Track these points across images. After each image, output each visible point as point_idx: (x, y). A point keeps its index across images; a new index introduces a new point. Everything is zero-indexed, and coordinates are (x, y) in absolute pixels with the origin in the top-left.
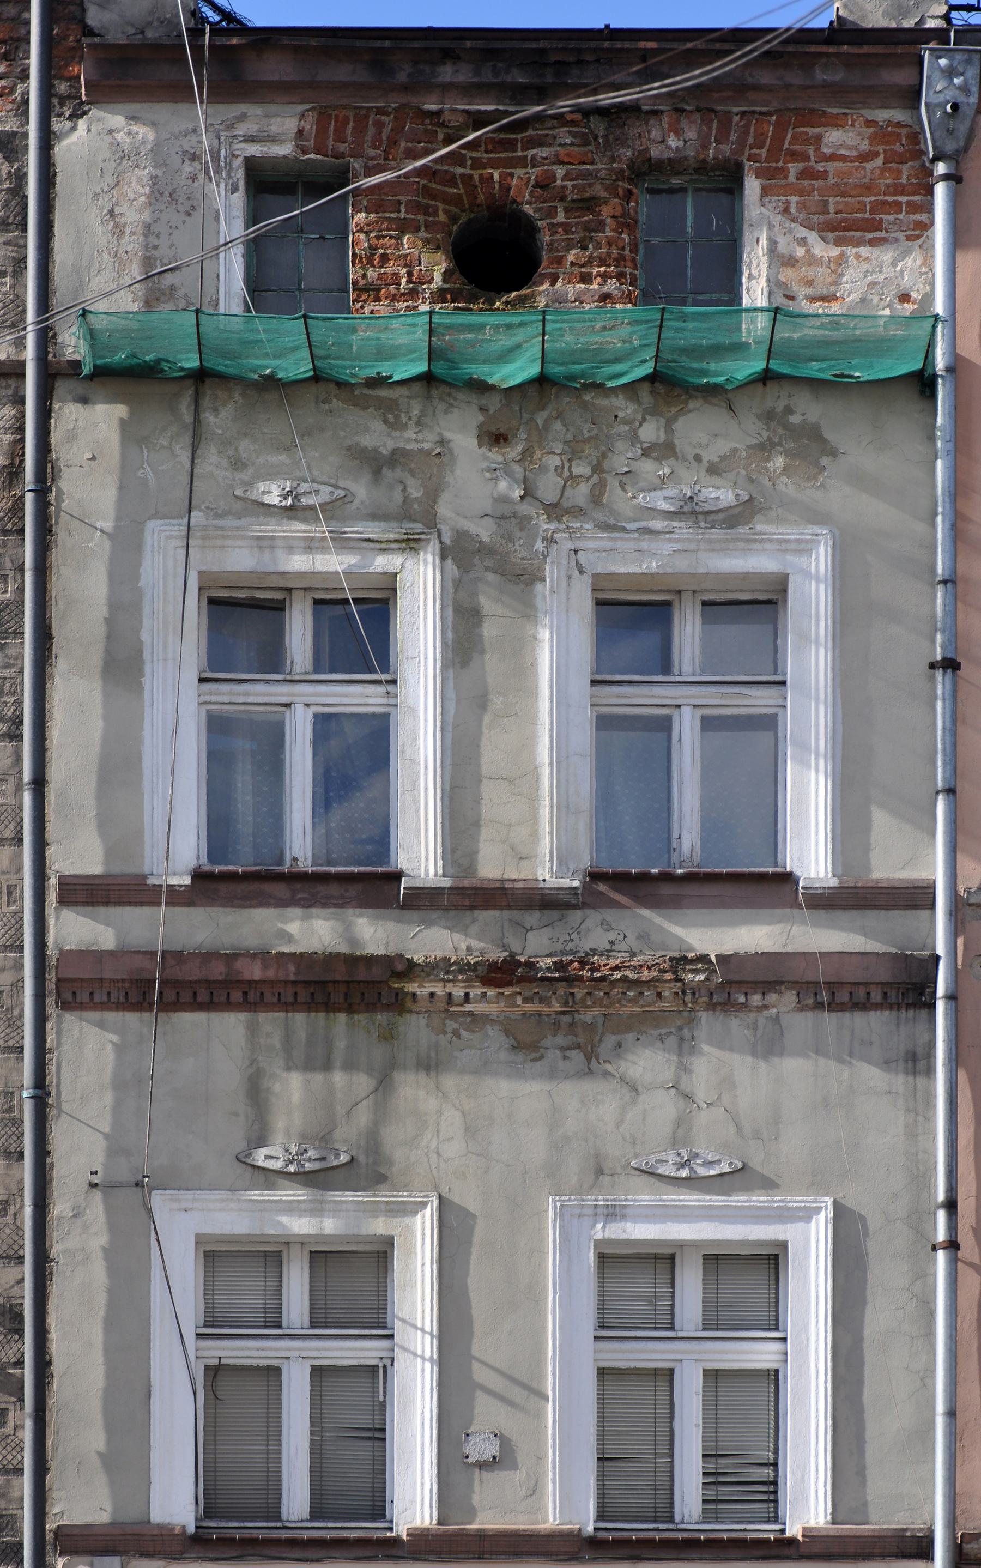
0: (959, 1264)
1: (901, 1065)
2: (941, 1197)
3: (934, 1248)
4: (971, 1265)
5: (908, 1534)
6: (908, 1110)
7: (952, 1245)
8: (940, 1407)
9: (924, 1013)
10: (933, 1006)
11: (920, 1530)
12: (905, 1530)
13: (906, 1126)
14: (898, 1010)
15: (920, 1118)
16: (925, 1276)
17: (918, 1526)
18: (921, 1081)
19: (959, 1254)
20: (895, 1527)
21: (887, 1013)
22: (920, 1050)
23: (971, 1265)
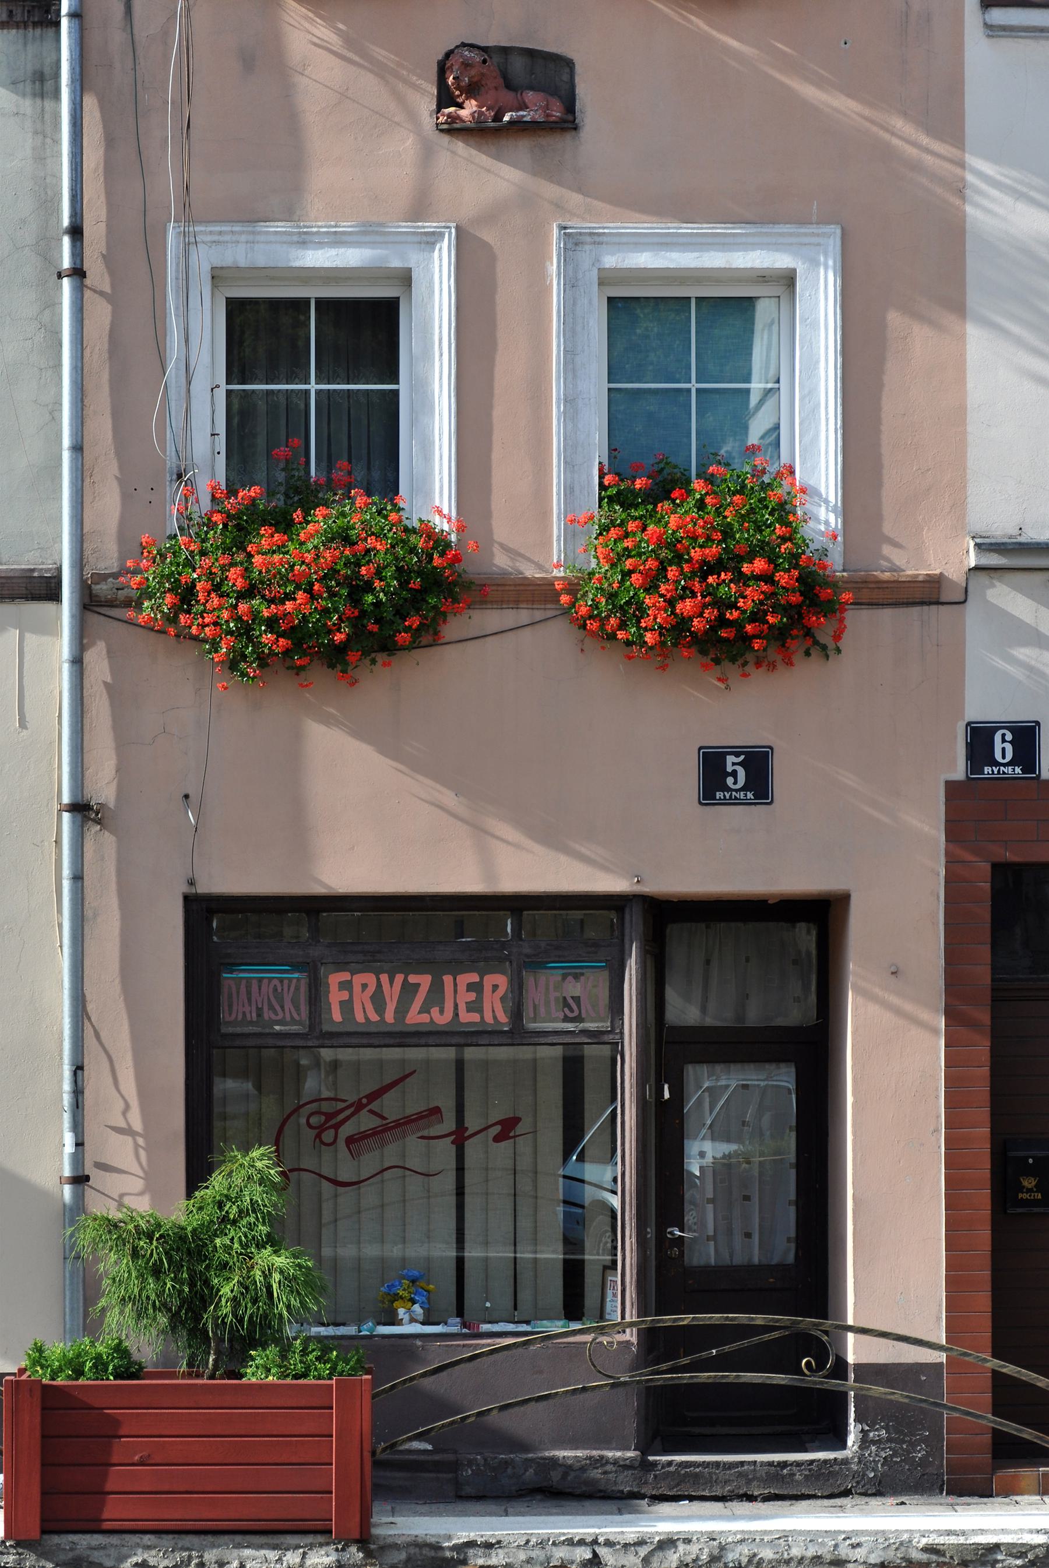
0: (88, 294)
1: (29, 88)
2: (66, 222)
3: (60, 276)
4: (102, 293)
5: (36, 574)
6: (36, 133)
7: (78, 273)
8: (66, 442)
9: (51, 32)
10: (57, 24)
11: (48, 570)
12: (33, 570)
13: (34, 149)
14: (25, 28)
15: (48, 141)
16: (54, 305)
17: (46, 566)
18: (48, 104)
19: (88, 281)
20: (23, 567)
21: (14, 31)
22: (47, 70)
23: (102, 293)
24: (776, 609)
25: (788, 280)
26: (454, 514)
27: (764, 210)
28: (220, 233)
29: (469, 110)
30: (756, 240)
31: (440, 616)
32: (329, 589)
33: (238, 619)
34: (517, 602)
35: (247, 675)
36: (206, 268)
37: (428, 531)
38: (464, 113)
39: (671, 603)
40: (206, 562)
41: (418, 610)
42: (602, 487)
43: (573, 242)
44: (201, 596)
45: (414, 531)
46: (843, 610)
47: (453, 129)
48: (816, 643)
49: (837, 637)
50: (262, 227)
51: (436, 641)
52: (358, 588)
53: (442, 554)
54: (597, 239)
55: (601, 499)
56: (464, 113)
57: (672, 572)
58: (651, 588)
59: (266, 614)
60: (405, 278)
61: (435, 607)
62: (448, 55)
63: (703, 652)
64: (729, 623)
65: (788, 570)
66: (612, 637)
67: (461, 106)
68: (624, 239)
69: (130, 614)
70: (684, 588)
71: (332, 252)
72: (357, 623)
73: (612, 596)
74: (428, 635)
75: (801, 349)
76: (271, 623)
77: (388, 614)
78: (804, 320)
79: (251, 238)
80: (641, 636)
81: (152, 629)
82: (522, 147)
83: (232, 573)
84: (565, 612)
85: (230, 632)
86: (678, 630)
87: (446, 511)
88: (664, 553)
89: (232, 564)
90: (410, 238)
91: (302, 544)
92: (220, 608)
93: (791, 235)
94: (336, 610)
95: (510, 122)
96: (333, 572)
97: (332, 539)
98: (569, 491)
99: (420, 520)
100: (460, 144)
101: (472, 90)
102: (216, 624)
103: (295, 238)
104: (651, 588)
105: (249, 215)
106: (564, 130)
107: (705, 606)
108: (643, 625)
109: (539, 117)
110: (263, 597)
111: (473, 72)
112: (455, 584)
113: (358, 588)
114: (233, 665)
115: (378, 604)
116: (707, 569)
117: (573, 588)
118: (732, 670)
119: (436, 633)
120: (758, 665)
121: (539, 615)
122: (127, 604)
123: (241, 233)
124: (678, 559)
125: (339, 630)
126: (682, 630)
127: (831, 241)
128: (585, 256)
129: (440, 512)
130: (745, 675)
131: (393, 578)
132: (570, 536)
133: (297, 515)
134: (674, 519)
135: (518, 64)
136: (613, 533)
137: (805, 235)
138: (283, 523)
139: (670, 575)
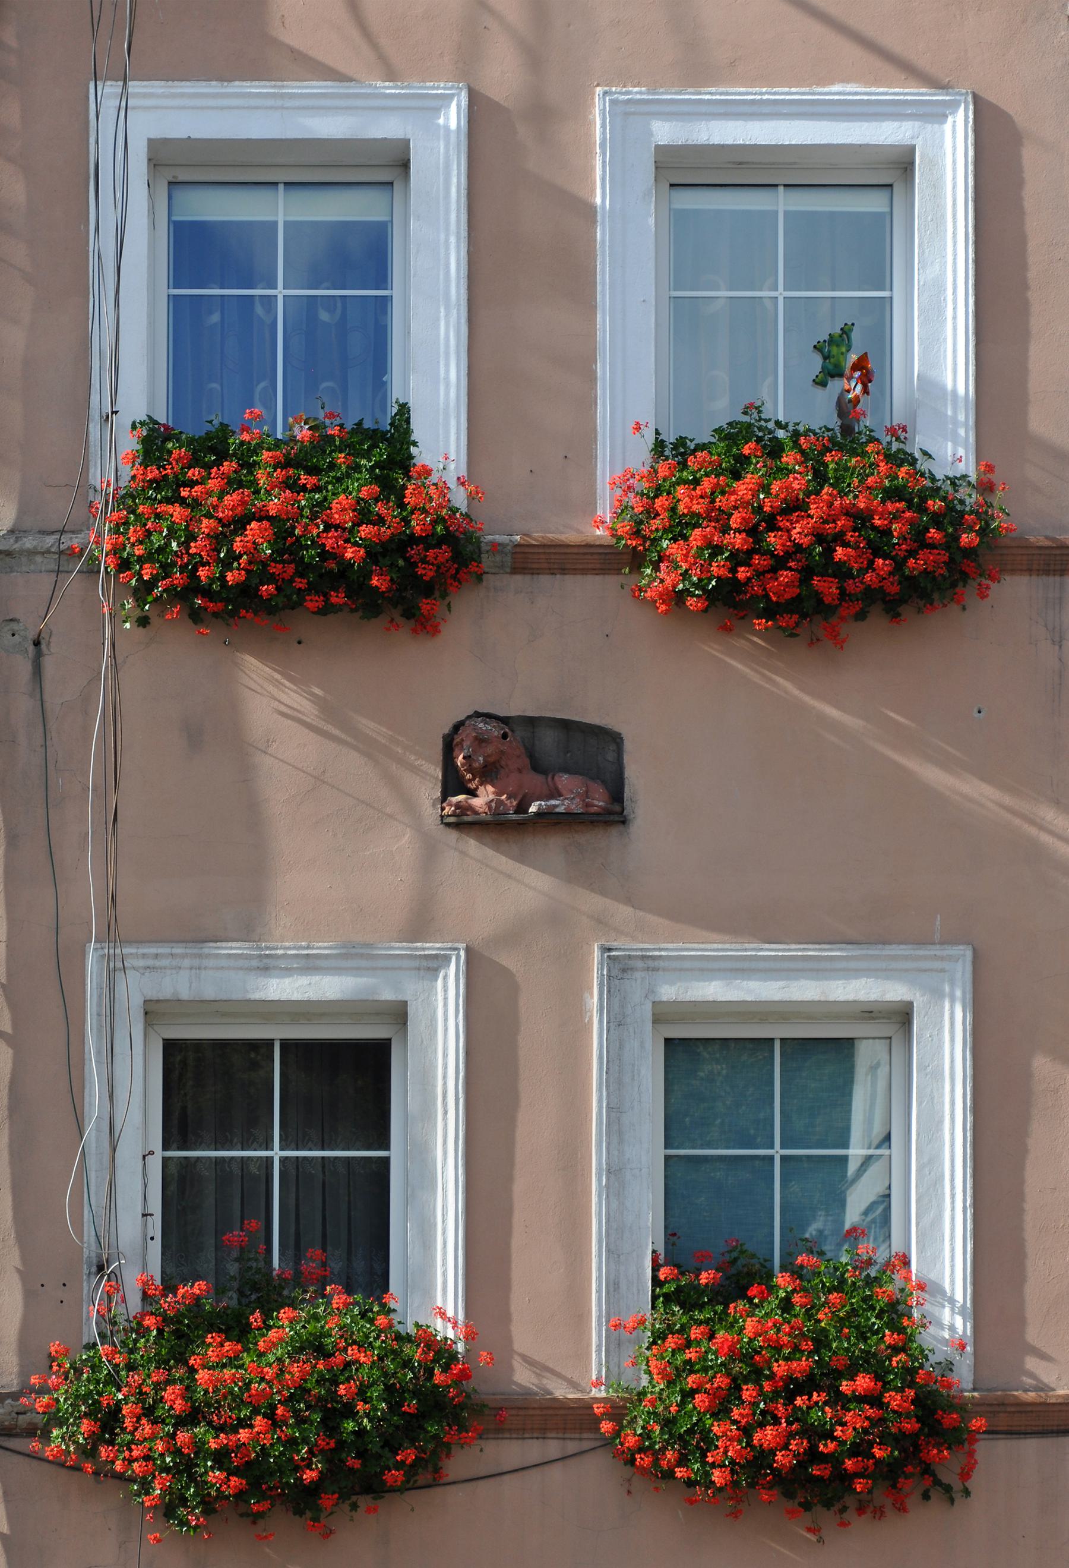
24: (884, 1439)
25: (902, 1017)
26: (461, 1317)
27: (871, 927)
28: (156, 956)
29: (484, 798)
30: (863, 965)
31: (442, 1448)
32: (296, 1413)
33: (177, 1452)
34: (544, 1430)
35: (187, 1523)
36: (137, 1002)
37: (426, 1339)
38: (478, 802)
39: (746, 1431)
40: (135, 1378)
41: (413, 1441)
42: (656, 1282)
43: (620, 968)
44: (128, 1423)
45: (409, 1338)
46: (972, 1440)
47: (463, 823)
48: (937, 1482)
49: (965, 1475)
50: (210, 948)
51: (437, 1480)
52: (335, 1413)
53: (446, 1368)
54: (651, 964)
55: (654, 1298)
56: (478, 802)
57: (748, 1392)
58: (720, 1412)
59: (213, 1446)
60: (399, 1014)
61: (436, 1437)
62: (457, 727)
63: (789, 1495)
64: (823, 1458)
65: (901, 1390)
66: (669, 1475)
67: (473, 793)
68: (687, 964)
69: (34, 1445)
70: (763, 1413)
71: (303, 981)
72: (333, 1458)
73: (668, 1423)
74: (427, 1473)
75: (919, 1104)
76: (220, 1458)
77: (374, 1445)
78: (922, 1068)
79: (196, 962)
80: (707, 1474)
81: (63, 1465)
82: (554, 846)
83: (169, 1393)
84: (607, 1443)
85: (166, 1469)
86: (756, 1465)
87: (450, 1313)
88: (737, 1368)
89: (169, 1382)
90: (406, 963)
91: (261, 1355)
92: (153, 1437)
93: (906, 958)
94: (305, 1440)
95: (538, 814)
96: (302, 1391)
97: (301, 1349)
98: (613, 1287)
99: (417, 1325)
100: (472, 842)
101: (488, 773)
102: (147, 1458)
103: (255, 963)
104: (720, 1412)
105: (195, 934)
106: (608, 824)
107: (791, 1435)
108: (710, 1459)
109: (576, 807)
110: (210, 1423)
111: (490, 750)
112: (462, 1406)
113: (335, 1413)
114: (169, 1509)
115: (361, 1433)
116: (793, 1388)
117: (617, 1412)
118: (826, 1517)
119: (437, 1470)
120: (861, 1511)
121: (572, 1447)
122: (30, 1432)
123: (184, 956)
124: (756, 1374)
125: (309, 1466)
126: (761, 1467)
127: (959, 966)
128: (636, 986)
129: (442, 1314)
130: (843, 1524)
131: (380, 1399)
132: (614, 1345)
133: (255, 1319)
134: (752, 1324)
135: (548, 740)
136: (671, 1342)
137: (925, 958)
138: (237, 1329)
139: (745, 1395)
